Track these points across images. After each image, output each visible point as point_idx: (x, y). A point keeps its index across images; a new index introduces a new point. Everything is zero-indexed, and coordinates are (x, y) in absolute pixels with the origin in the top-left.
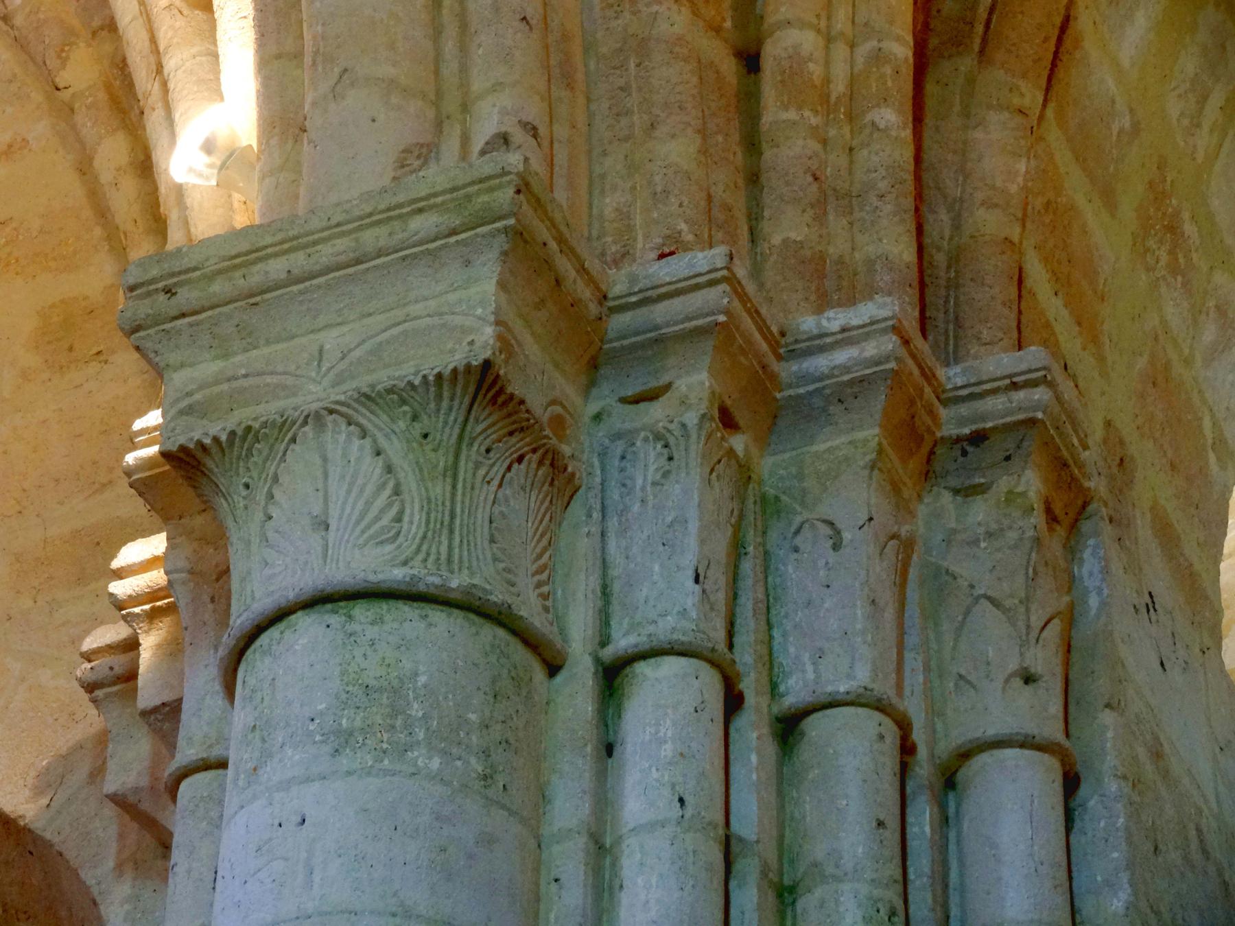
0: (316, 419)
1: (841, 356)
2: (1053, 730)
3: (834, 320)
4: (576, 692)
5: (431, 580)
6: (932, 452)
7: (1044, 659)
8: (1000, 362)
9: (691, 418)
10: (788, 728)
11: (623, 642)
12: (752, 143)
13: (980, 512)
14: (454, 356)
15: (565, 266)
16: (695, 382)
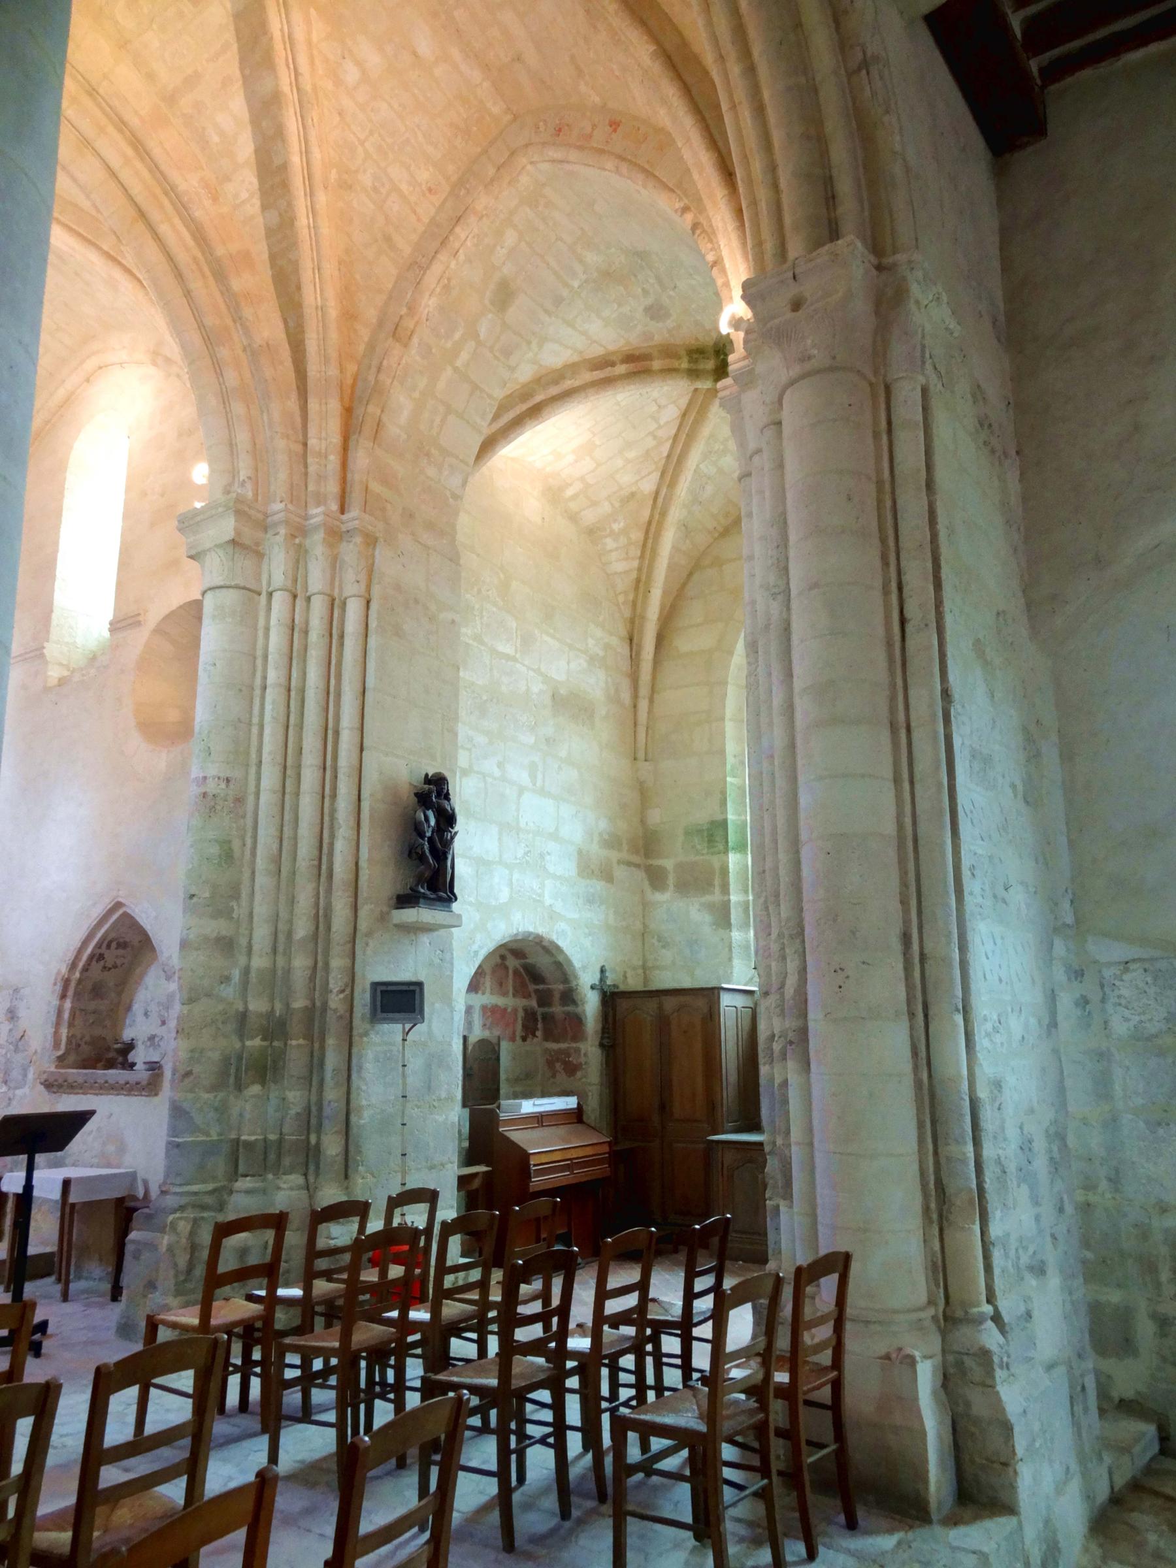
0: (209, 550)
4: (263, 599)
5: (228, 583)
6: (336, 535)
13: (351, 546)
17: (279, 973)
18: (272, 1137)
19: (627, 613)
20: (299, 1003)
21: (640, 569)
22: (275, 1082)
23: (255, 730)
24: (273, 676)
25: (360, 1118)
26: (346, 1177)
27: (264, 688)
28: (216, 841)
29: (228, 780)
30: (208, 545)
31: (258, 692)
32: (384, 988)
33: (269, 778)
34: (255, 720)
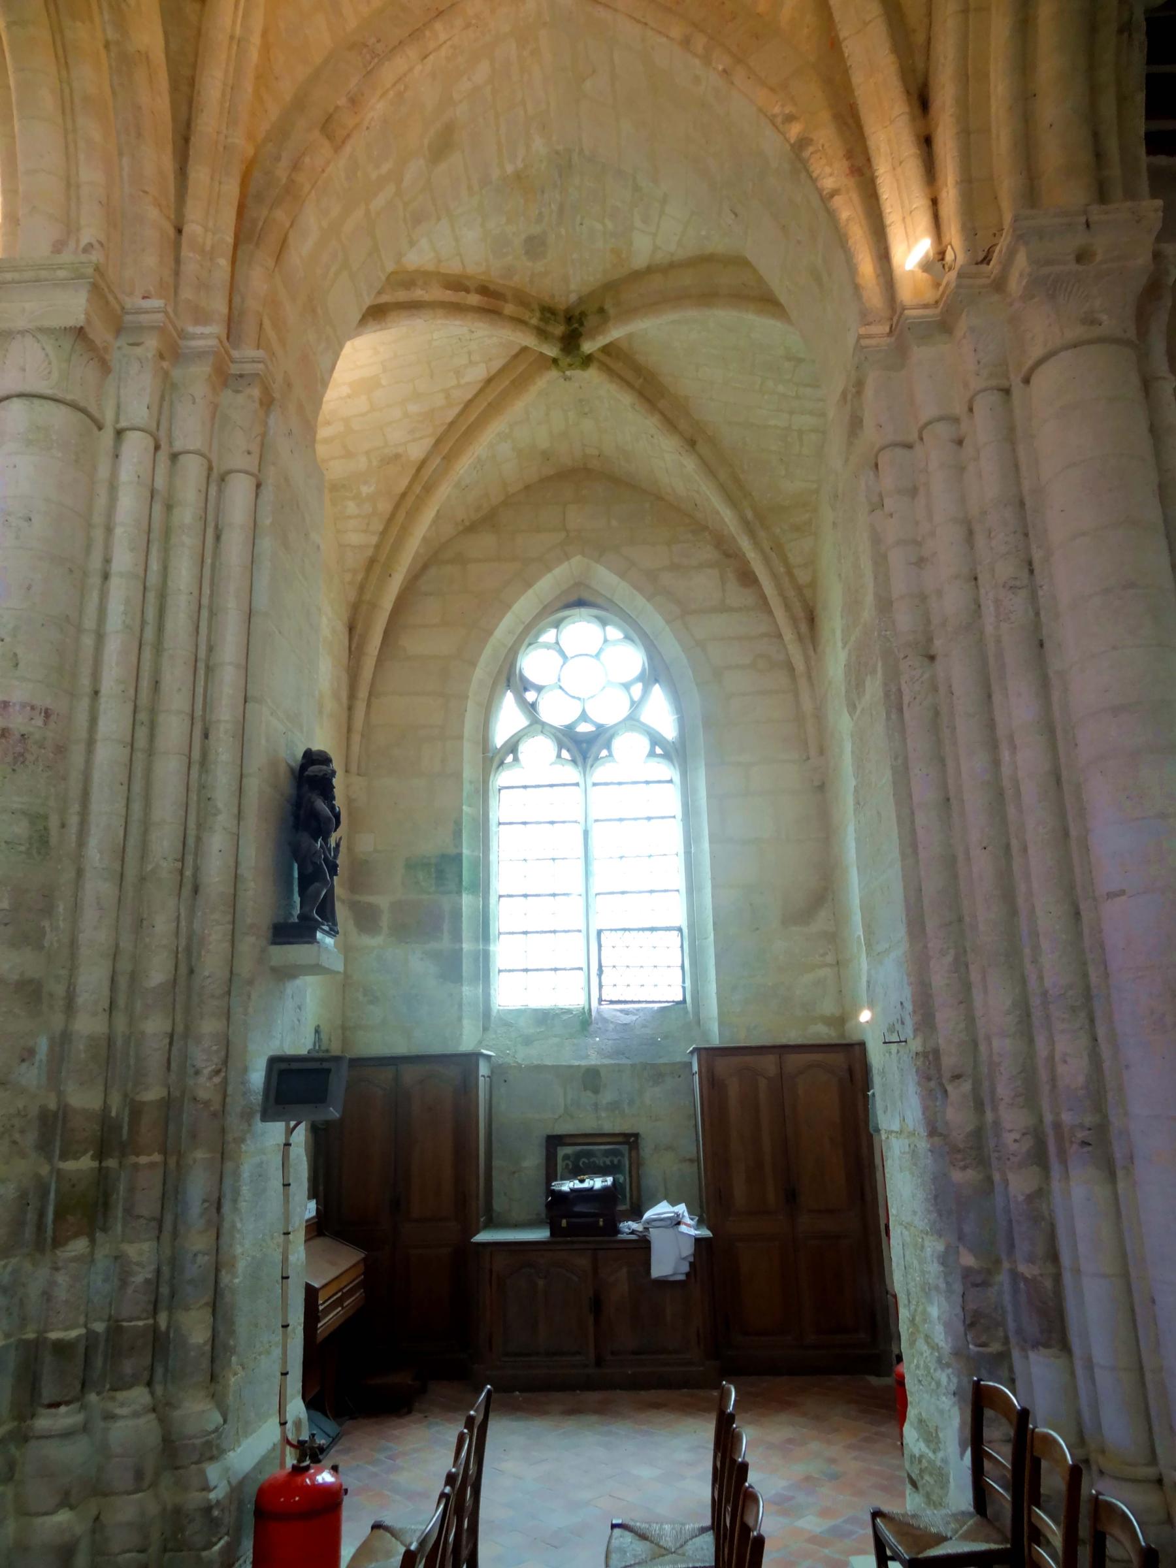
0: (23, 333)
1: (201, 343)
2: (255, 470)
3: (199, 330)
4: (108, 436)
5: (60, 395)
6: (226, 377)
7: (255, 449)
8: (250, 352)
9: (150, 355)
10: (174, 457)
11: (123, 424)
12: (177, 260)
13: (240, 399)
14: (71, 323)
15: (111, 298)
16: (152, 343)
17: (119, 1042)
18: (99, 1327)
19: (352, 596)
20: (153, 1094)
21: (378, 547)
22: (105, 1230)
23: (88, 641)
24: (123, 560)
25: (234, 1275)
26: (213, 1378)
27: (106, 576)
28: (24, 813)
29: (47, 714)
30: (21, 324)
31: (95, 580)
32: (284, 1066)
33: (113, 721)
34: (89, 623)
